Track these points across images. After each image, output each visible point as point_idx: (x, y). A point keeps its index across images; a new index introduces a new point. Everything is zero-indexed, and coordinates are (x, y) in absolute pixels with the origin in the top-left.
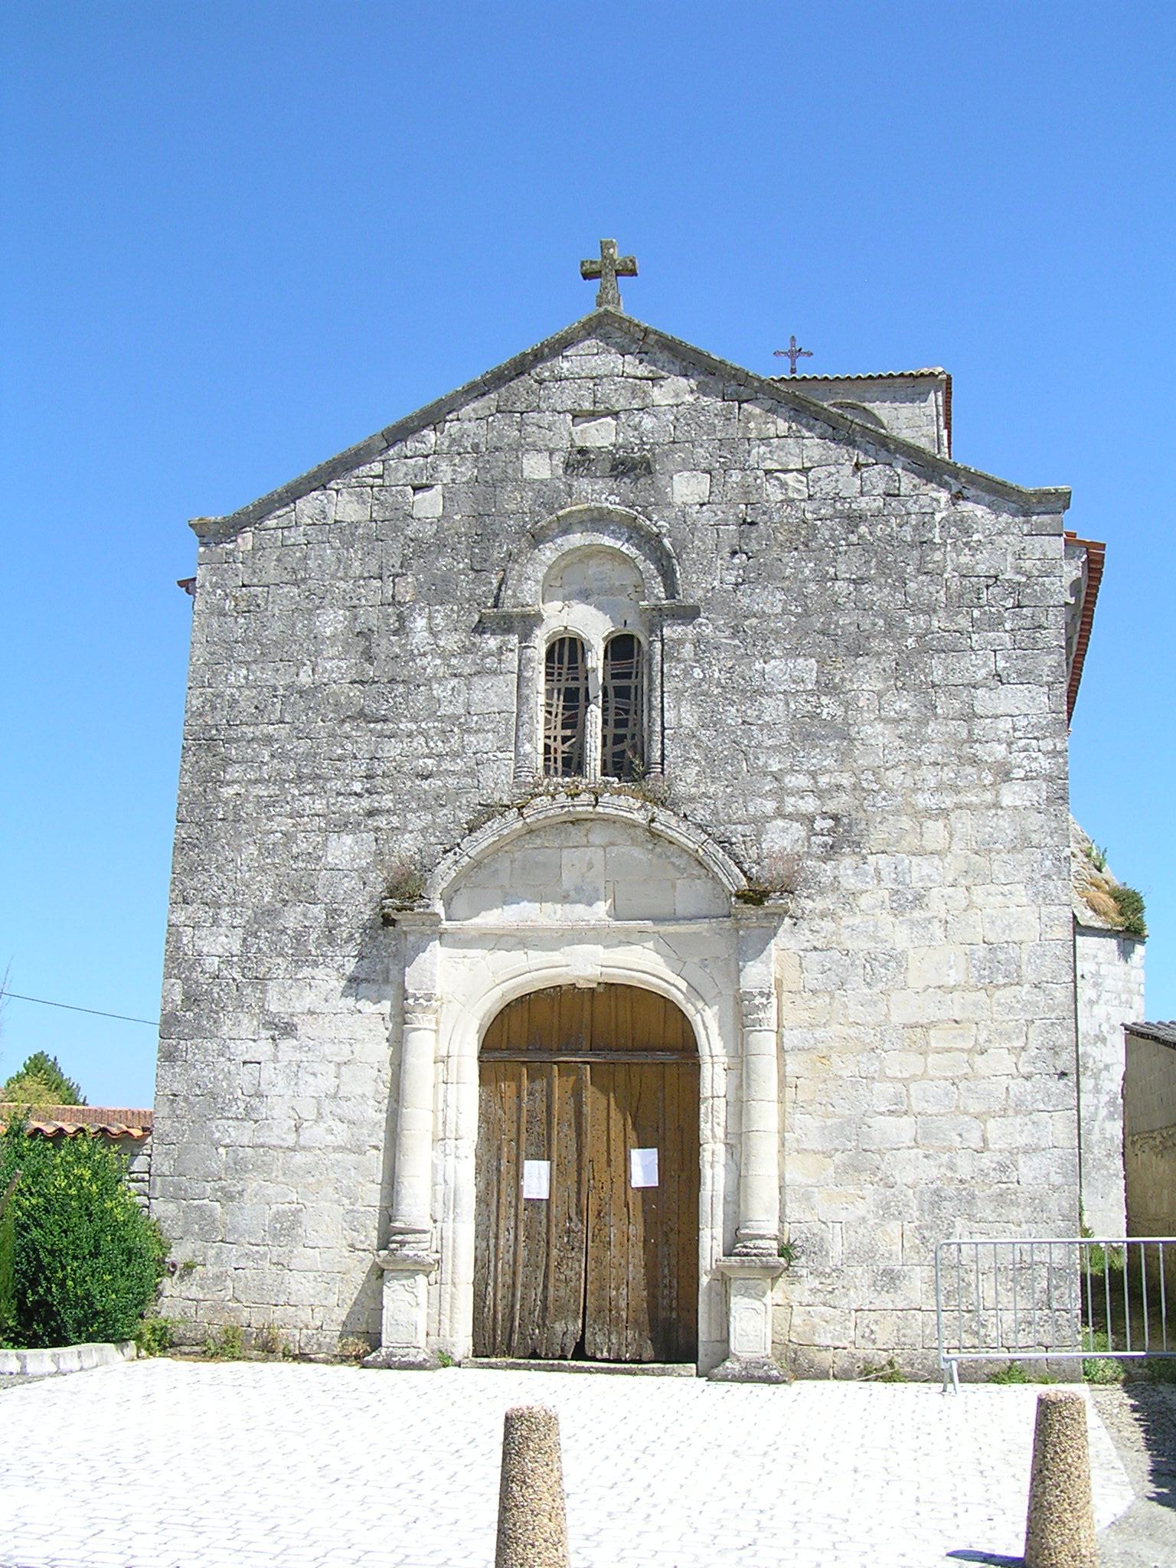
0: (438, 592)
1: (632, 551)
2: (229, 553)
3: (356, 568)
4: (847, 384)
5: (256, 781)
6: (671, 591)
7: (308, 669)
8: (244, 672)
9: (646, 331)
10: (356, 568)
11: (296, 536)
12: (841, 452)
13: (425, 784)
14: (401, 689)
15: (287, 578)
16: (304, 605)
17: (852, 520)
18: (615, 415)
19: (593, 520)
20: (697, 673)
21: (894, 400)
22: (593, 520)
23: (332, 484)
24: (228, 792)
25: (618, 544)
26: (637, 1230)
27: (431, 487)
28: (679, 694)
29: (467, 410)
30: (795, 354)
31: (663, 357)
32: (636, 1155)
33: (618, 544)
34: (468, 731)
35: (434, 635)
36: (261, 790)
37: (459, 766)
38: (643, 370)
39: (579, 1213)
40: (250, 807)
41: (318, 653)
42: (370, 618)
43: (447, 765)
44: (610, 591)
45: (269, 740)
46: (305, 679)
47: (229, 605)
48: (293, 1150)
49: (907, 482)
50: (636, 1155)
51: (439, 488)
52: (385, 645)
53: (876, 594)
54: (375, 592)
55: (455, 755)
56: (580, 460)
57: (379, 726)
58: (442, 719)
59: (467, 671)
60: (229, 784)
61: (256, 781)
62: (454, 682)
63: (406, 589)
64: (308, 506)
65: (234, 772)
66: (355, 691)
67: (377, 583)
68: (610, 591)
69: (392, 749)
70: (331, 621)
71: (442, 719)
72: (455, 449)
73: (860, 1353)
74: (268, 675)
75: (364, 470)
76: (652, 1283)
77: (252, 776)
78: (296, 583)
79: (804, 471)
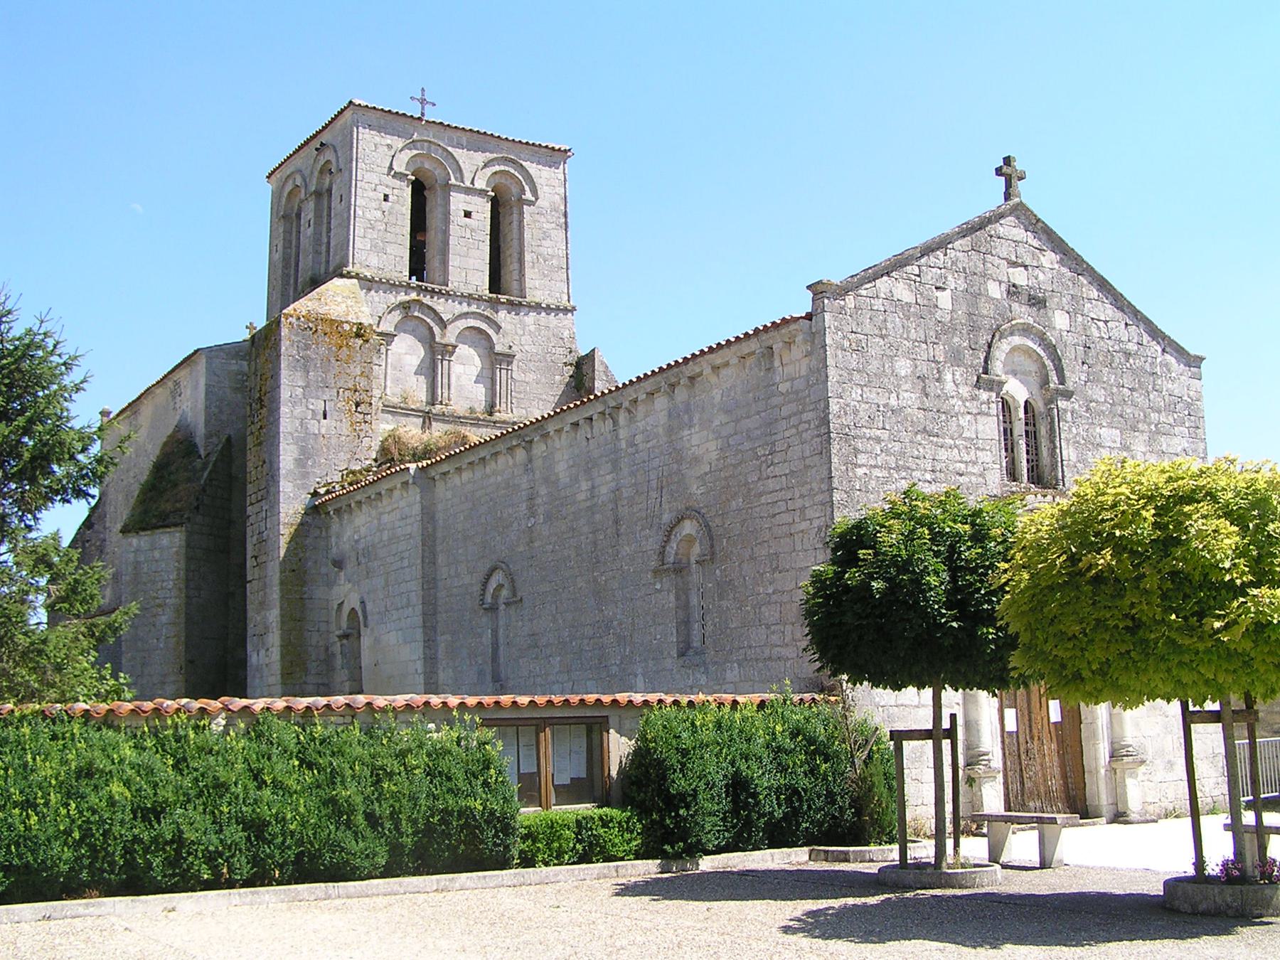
0: (956, 358)
1: (1040, 351)
2: (842, 308)
3: (913, 335)
4: (510, 144)
5: (875, 467)
6: (1062, 380)
7: (894, 395)
8: (859, 392)
9: (1038, 220)
10: (913, 335)
11: (878, 304)
12: (1119, 314)
13: (961, 479)
14: (943, 417)
15: (877, 332)
16: (888, 352)
17: (1128, 355)
18: (1026, 267)
19: (1024, 330)
20: (1074, 430)
21: (539, 163)
22: (1024, 330)
23: (893, 274)
24: (860, 471)
25: (1035, 347)
26: (1054, 746)
27: (944, 289)
28: (1068, 440)
29: (957, 244)
30: (423, 102)
31: (1044, 237)
32: (1051, 703)
33: (1035, 347)
34: (978, 449)
35: (957, 385)
36: (877, 472)
37: (975, 470)
38: (1036, 243)
39: (1032, 738)
40: (873, 483)
41: (899, 386)
42: (923, 368)
43: (970, 469)
44: (1024, 373)
45: (878, 440)
46: (893, 402)
47: (846, 344)
48: (917, 707)
49: (1146, 338)
50: (1051, 703)
51: (948, 291)
52: (933, 388)
53: (1139, 398)
54: (923, 352)
55: (975, 463)
56: (1013, 291)
57: (935, 439)
58: (965, 439)
59: (975, 411)
60: (860, 466)
61: (875, 467)
62: (969, 417)
63: (940, 352)
64: (883, 284)
65: (862, 459)
66: (921, 414)
67: (924, 346)
68: (1024, 373)
69: (943, 454)
70: (903, 366)
71: (965, 439)
72: (954, 267)
73: (1163, 805)
74: (873, 395)
75: (909, 269)
76: (1064, 776)
77: (872, 462)
78: (882, 337)
79: (1106, 322)
